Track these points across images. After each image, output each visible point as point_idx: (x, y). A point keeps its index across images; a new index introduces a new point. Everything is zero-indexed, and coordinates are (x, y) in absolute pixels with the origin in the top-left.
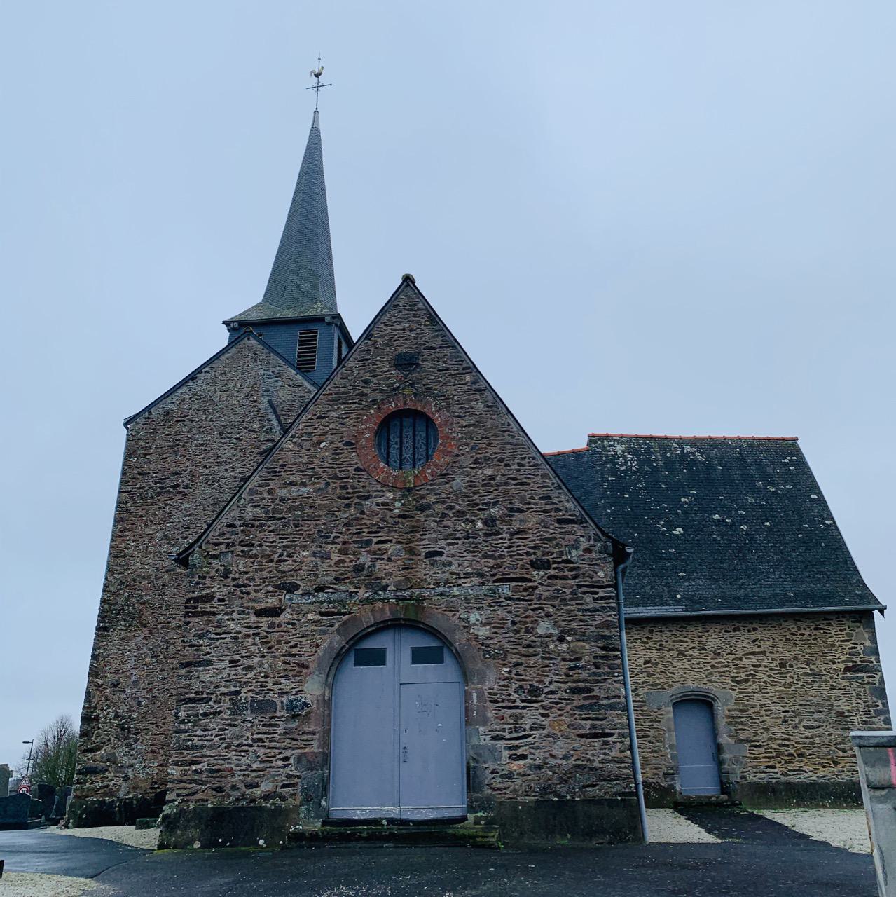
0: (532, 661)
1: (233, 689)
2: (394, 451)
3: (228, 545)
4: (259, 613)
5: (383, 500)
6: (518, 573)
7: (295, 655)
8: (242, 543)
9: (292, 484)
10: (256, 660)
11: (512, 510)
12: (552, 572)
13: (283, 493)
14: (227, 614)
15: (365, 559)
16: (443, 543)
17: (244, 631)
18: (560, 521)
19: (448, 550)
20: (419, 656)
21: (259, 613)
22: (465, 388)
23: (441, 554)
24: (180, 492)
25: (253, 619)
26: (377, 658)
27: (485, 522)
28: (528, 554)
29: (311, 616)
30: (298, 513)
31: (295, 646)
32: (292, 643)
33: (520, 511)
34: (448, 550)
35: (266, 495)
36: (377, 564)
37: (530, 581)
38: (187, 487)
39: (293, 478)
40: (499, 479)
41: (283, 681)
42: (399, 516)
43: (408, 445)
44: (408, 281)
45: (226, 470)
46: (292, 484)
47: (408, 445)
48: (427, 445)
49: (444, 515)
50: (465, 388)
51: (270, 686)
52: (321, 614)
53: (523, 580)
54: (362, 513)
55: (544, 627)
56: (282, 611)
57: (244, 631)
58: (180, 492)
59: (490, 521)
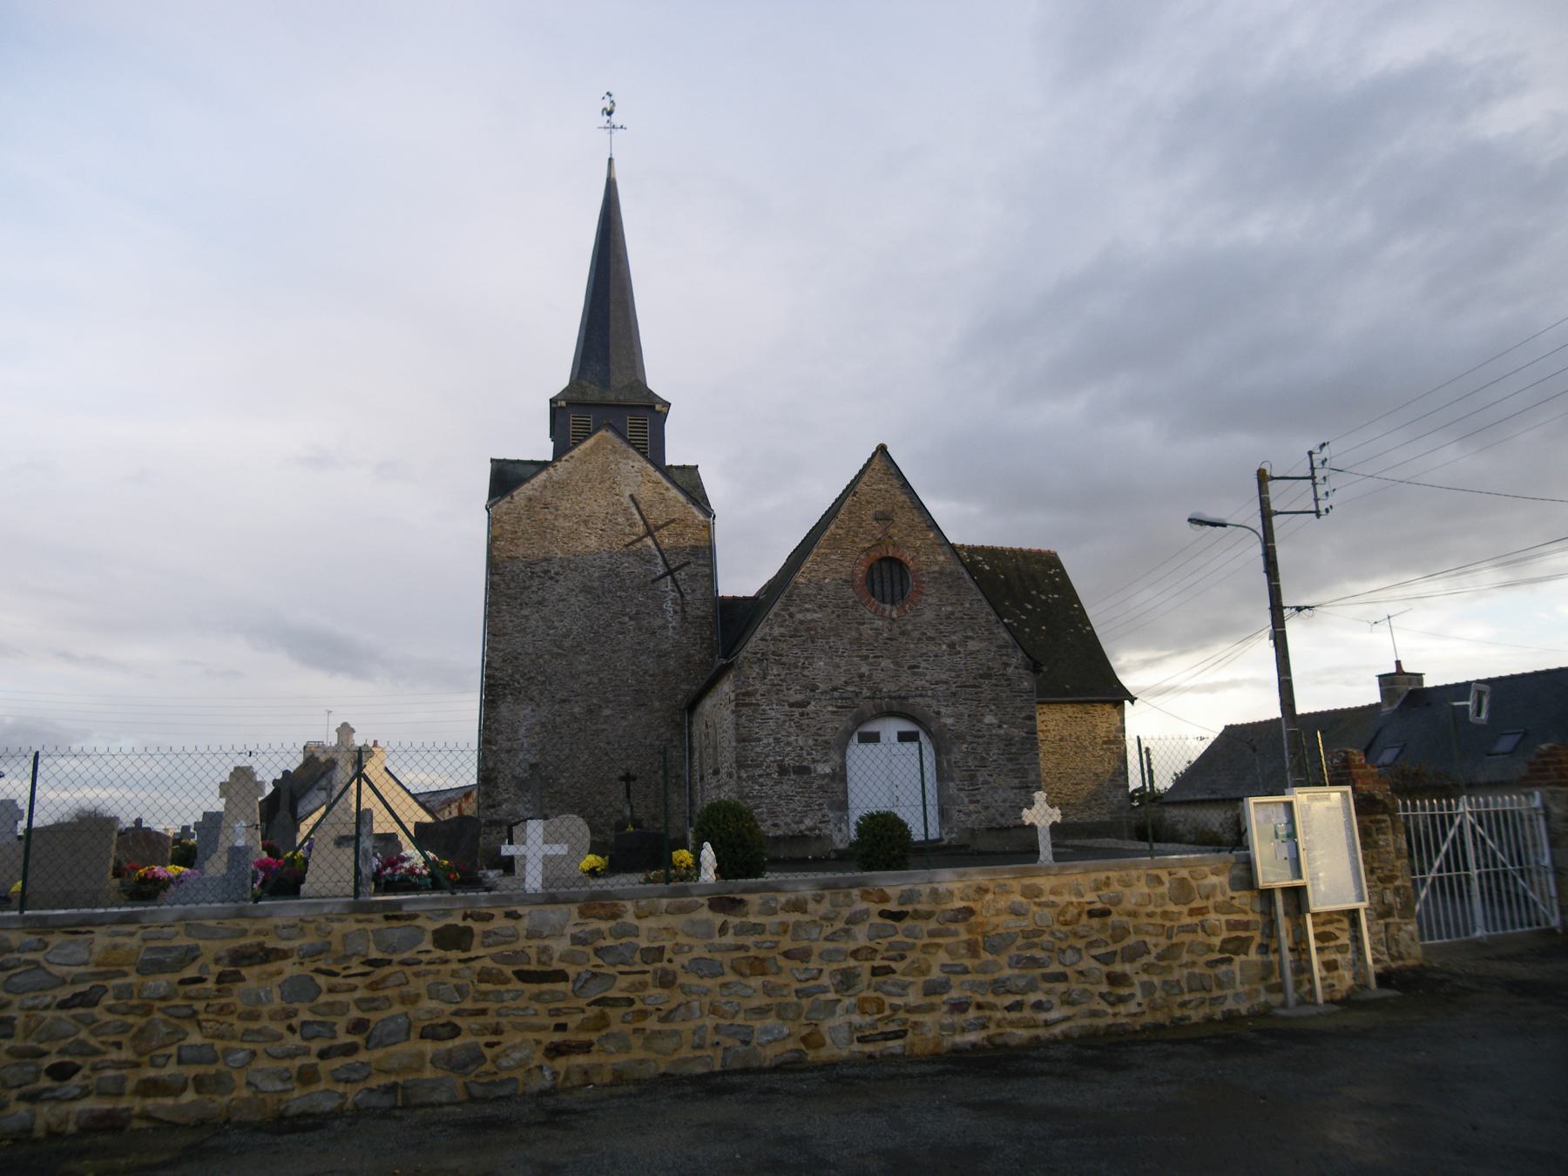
0: (981, 740)
1: (778, 758)
2: (877, 588)
3: (763, 654)
4: (791, 705)
5: (875, 626)
6: (972, 682)
7: (820, 735)
8: (774, 653)
9: (808, 610)
10: (793, 738)
11: (967, 637)
12: (994, 681)
13: (800, 616)
14: (768, 705)
15: (865, 669)
16: (920, 659)
17: (783, 718)
18: (999, 647)
19: (923, 665)
20: (903, 737)
21: (791, 705)
22: (929, 542)
23: (918, 667)
24: (551, 578)
25: (787, 708)
26: (874, 738)
27: (949, 646)
28: (978, 669)
29: (830, 708)
30: (812, 632)
31: (820, 729)
32: (818, 726)
33: (972, 638)
34: (923, 665)
35: (787, 617)
36: (874, 672)
37: (979, 687)
38: (557, 573)
39: (807, 606)
40: (957, 615)
41: (814, 752)
42: (888, 639)
43: (887, 585)
44: (882, 449)
45: (595, 560)
46: (808, 610)
47: (887, 585)
48: (902, 585)
49: (920, 639)
50: (929, 542)
51: (805, 755)
52: (837, 707)
53: (974, 686)
54: (861, 635)
55: (989, 719)
56: (809, 703)
57: (783, 718)
58: (551, 578)
59: (952, 646)
